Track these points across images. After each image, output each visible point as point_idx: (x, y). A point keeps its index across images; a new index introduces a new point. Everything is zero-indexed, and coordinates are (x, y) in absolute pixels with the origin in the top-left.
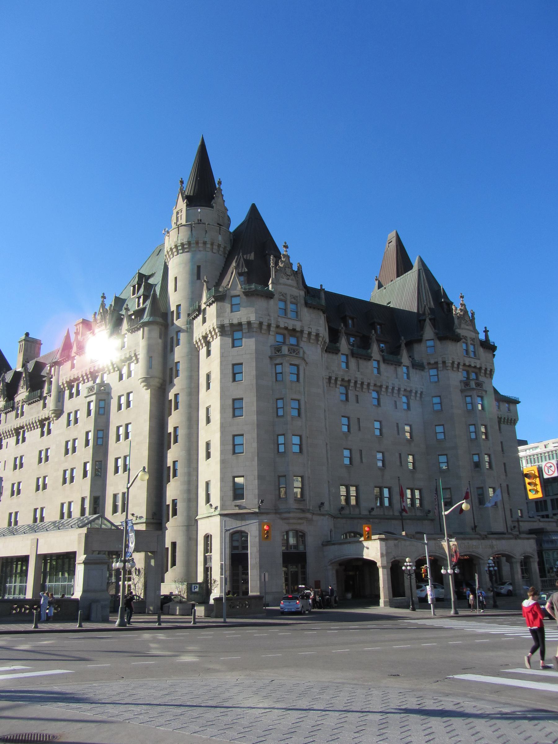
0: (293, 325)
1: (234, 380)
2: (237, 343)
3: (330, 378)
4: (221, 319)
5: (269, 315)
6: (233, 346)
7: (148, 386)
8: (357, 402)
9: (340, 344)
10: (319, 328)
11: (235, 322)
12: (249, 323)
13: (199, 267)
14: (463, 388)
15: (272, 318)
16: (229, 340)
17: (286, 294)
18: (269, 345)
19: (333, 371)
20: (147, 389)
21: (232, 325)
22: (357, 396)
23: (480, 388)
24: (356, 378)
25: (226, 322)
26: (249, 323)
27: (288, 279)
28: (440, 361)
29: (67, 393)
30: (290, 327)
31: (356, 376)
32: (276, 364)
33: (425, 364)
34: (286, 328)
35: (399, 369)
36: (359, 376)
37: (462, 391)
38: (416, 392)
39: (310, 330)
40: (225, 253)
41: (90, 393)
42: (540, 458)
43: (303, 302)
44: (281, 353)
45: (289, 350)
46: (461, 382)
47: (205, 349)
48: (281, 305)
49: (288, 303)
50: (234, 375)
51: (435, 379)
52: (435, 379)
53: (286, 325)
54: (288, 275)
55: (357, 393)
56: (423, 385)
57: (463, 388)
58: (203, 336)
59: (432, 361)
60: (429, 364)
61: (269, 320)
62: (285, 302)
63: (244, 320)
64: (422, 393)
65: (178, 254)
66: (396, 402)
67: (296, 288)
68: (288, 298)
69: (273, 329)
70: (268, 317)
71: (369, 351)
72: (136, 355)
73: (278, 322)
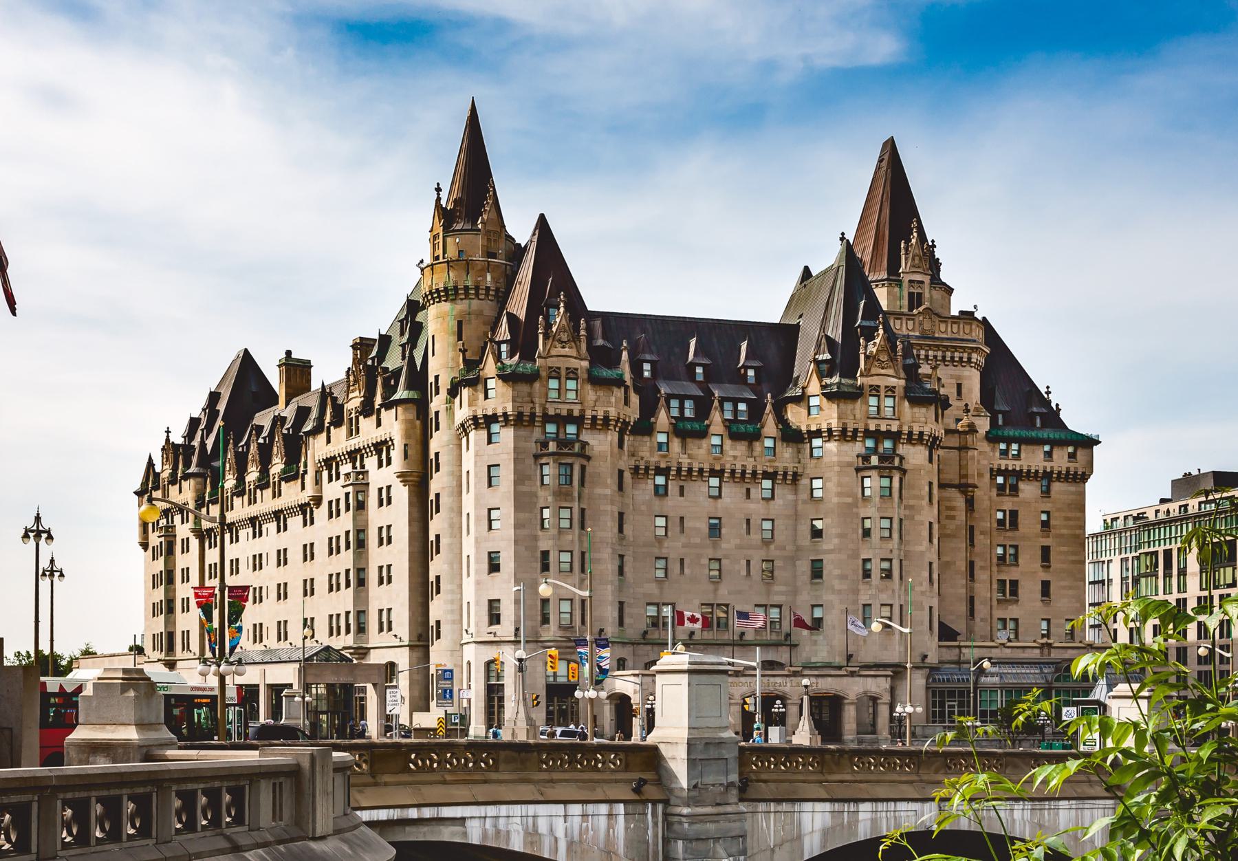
0: (568, 410)
1: (490, 485)
2: (494, 439)
3: (636, 468)
4: (474, 408)
5: (532, 402)
6: (489, 442)
7: (404, 482)
8: (682, 494)
9: (657, 418)
10: (609, 409)
12: (505, 415)
14: (861, 465)
15: (537, 405)
16: (484, 433)
17: (559, 368)
18: (534, 440)
19: (642, 458)
20: (405, 486)
21: (485, 416)
22: (682, 488)
23: (890, 463)
24: (680, 463)
25: (480, 413)
26: (505, 415)
27: (563, 347)
28: (824, 427)
29: (325, 474)
30: (564, 413)
31: (680, 460)
32: (542, 465)
33: (804, 429)
34: (558, 415)
35: (757, 445)
36: (685, 461)
37: (858, 470)
38: (785, 474)
39: (594, 413)
42: (1129, 538)
43: (586, 376)
46: (858, 456)
47: (465, 438)
48: (553, 384)
49: (563, 379)
50: (490, 478)
51: (715, 492)
52: (715, 492)
53: (558, 411)
55: (682, 483)
56: (799, 463)
57: (861, 465)
59: (813, 428)
60: (809, 432)
61: (531, 408)
62: (559, 378)
64: (795, 475)
65: (433, 304)
66: (748, 490)
67: (576, 358)
68: (563, 373)
70: (531, 405)
71: (706, 422)
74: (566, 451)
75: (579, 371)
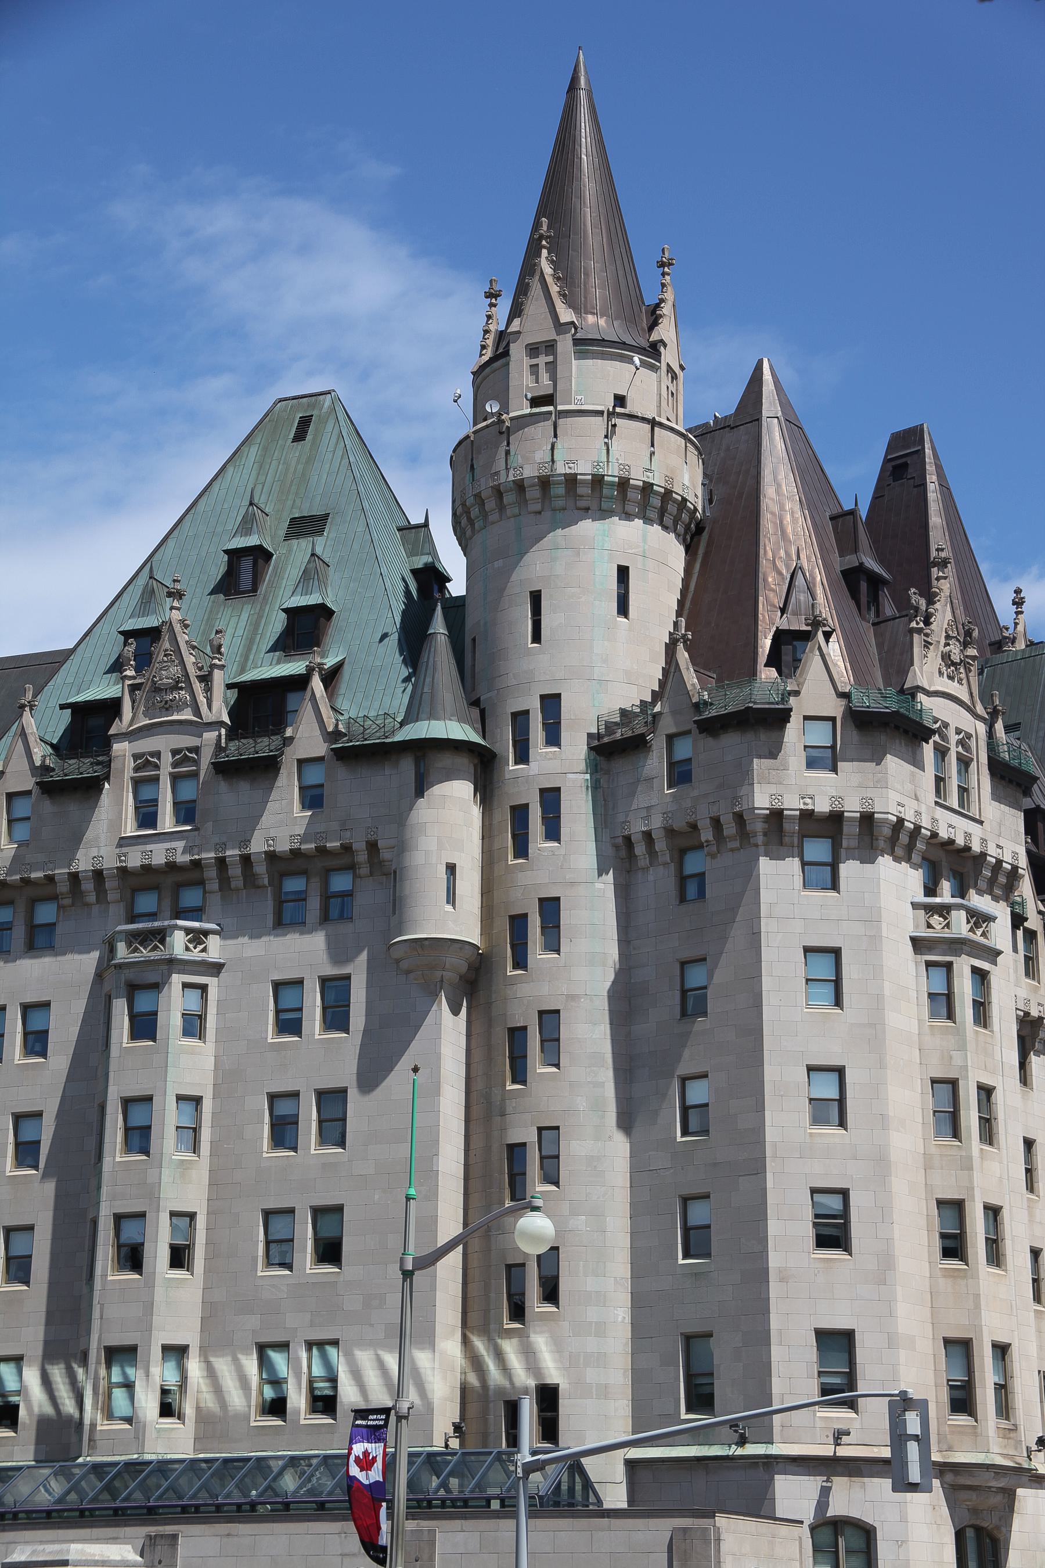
4: (773, 789)
11: (822, 806)
13: (623, 573)
21: (807, 815)
25: (792, 804)
40: (687, 528)
41: (136, 950)
44: (948, 925)
45: (968, 922)
54: (954, 664)
58: (670, 832)
61: (918, 813)
63: (852, 807)
69: (920, 846)
72: (373, 847)
73: (934, 820)
74: (977, 937)
75: (974, 739)
